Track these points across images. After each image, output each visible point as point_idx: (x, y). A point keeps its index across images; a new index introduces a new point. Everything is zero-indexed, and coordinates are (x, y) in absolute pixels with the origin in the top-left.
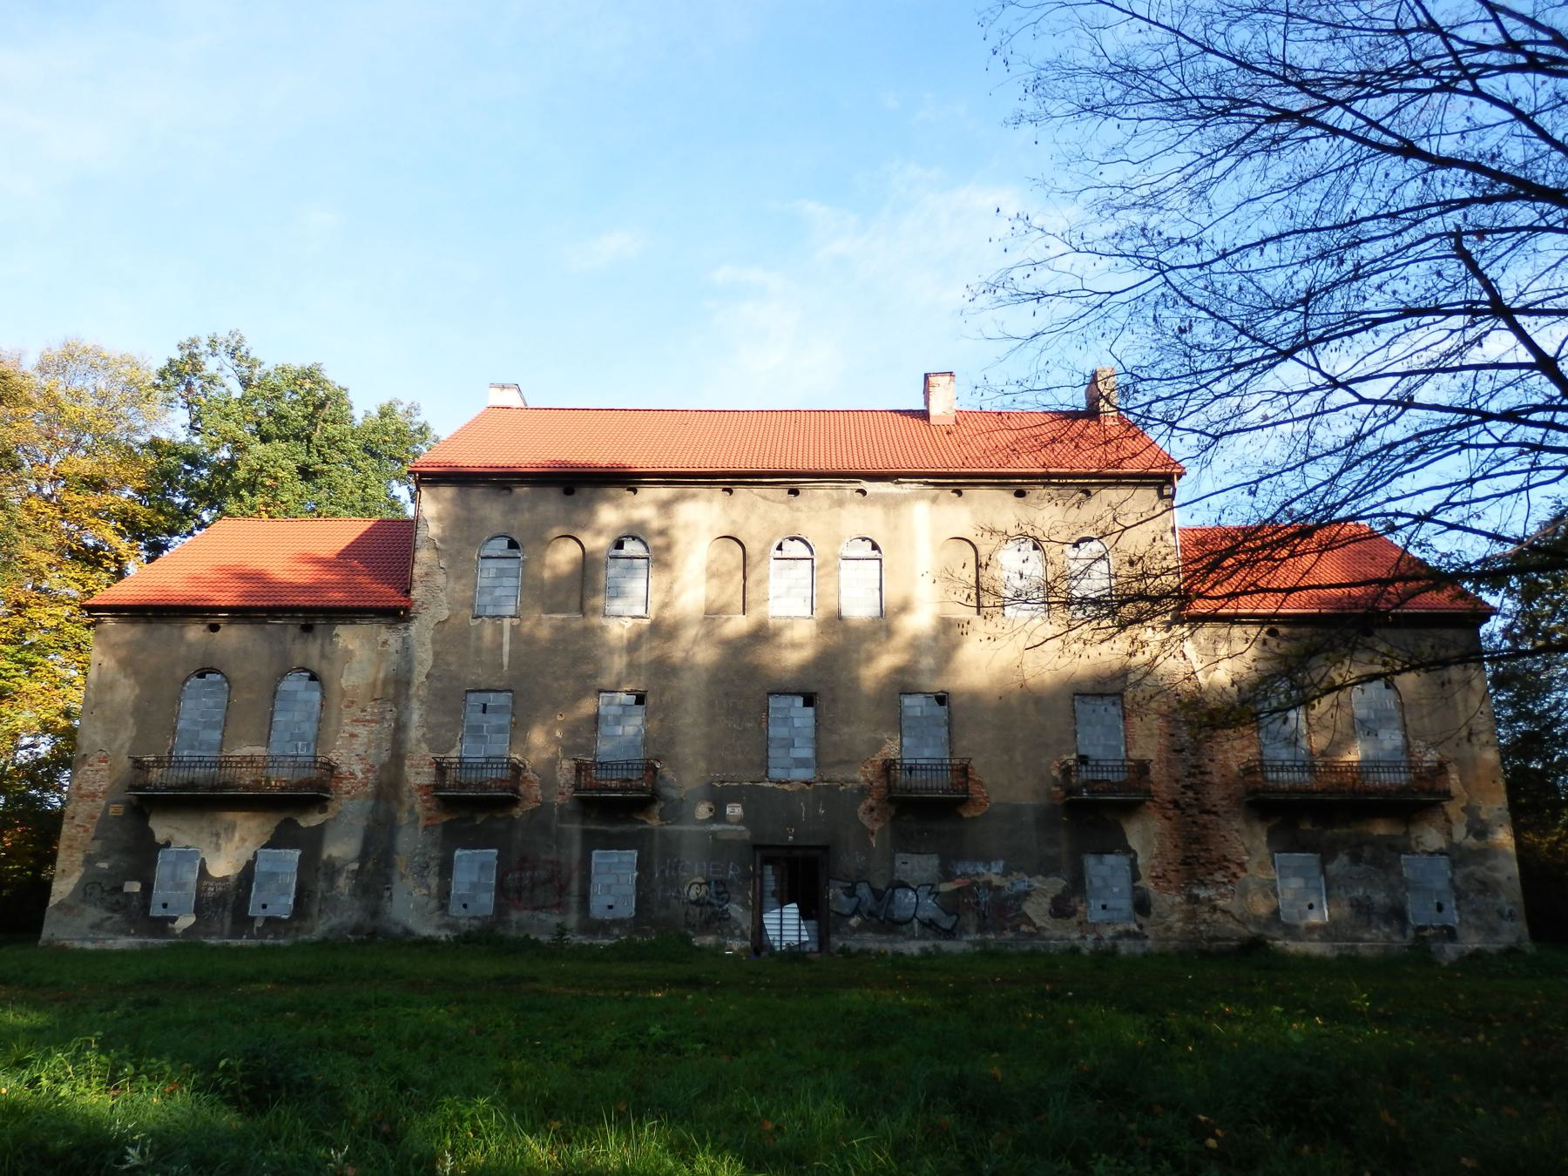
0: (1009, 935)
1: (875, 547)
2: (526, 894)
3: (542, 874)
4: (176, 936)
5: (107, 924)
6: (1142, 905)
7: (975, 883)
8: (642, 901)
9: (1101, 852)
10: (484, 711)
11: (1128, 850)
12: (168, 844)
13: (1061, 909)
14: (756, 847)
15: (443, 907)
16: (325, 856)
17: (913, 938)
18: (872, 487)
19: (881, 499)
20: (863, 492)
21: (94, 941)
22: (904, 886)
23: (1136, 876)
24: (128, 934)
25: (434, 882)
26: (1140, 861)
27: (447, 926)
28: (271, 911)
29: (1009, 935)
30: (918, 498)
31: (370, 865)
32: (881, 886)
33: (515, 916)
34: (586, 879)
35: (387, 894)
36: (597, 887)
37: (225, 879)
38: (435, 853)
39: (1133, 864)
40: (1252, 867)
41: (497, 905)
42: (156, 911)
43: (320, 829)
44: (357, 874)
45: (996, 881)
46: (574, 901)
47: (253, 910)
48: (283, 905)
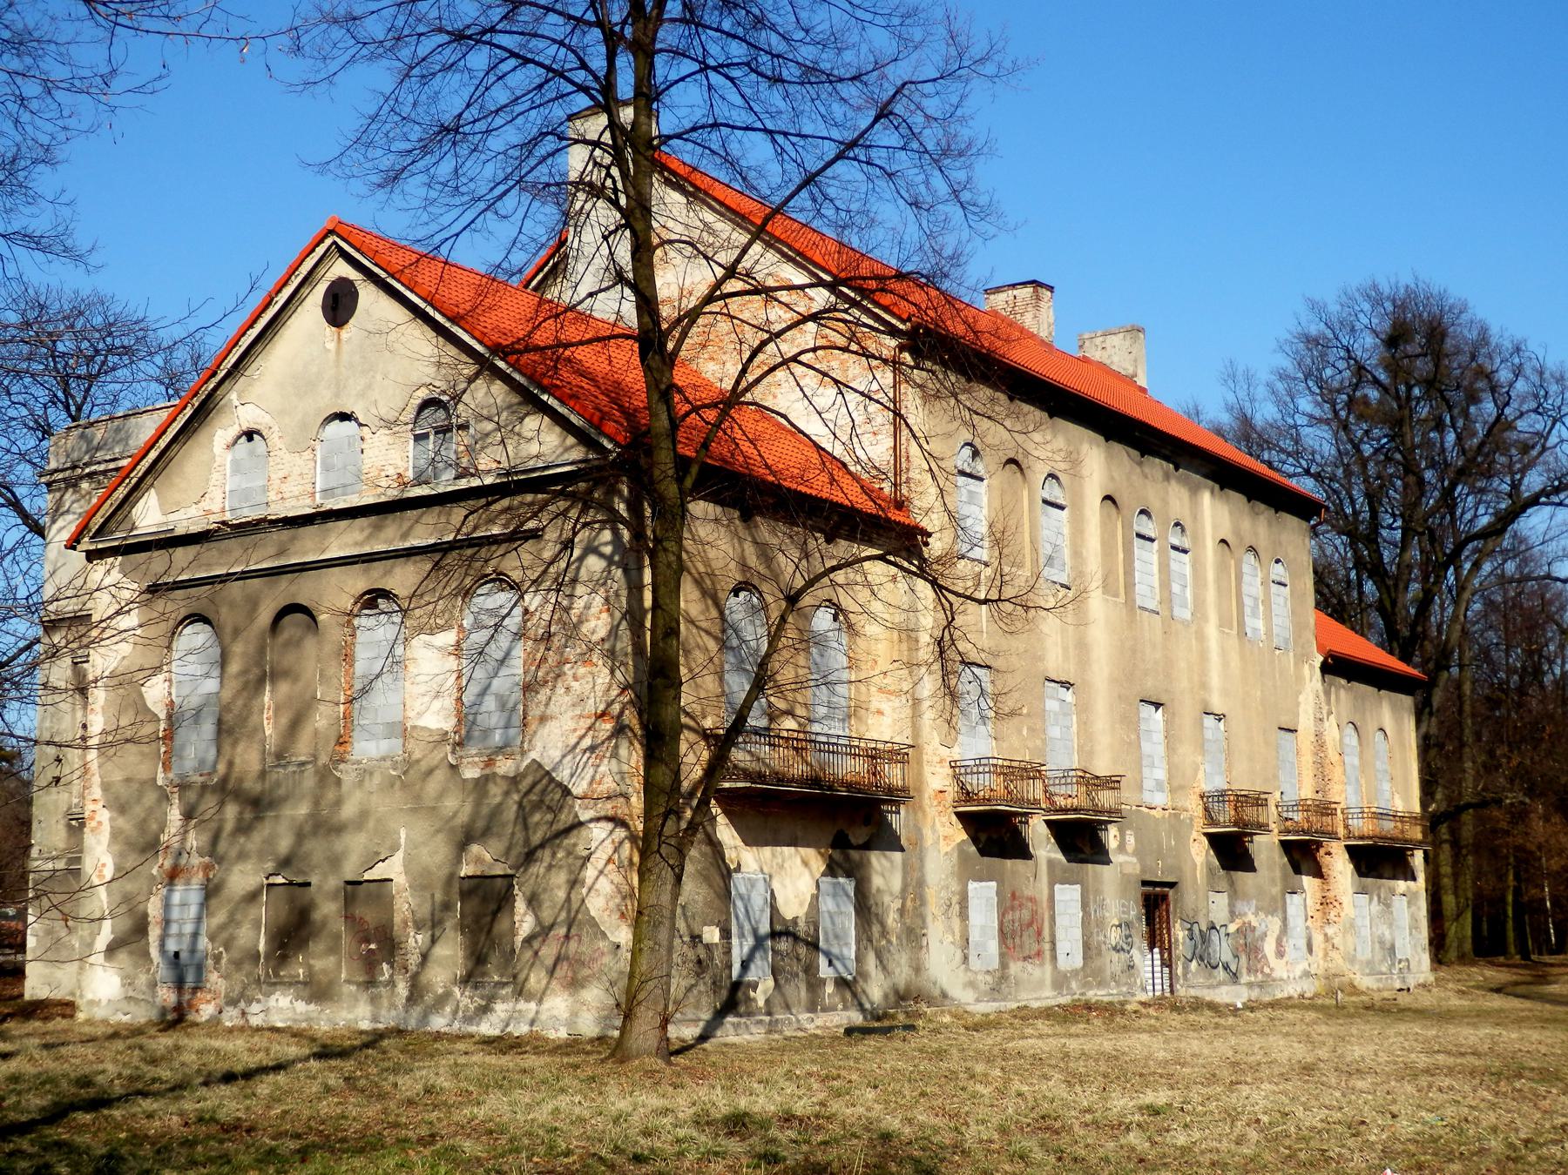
2: (1017, 940)
3: (1026, 914)
8: (1086, 946)
13: (1280, 954)
14: (1145, 883)
15: (966, 958)
33: (1015, 968)
36: (1060, 934)
38: (955, 887)
41: (1002, 955)
46: (1047, 946)
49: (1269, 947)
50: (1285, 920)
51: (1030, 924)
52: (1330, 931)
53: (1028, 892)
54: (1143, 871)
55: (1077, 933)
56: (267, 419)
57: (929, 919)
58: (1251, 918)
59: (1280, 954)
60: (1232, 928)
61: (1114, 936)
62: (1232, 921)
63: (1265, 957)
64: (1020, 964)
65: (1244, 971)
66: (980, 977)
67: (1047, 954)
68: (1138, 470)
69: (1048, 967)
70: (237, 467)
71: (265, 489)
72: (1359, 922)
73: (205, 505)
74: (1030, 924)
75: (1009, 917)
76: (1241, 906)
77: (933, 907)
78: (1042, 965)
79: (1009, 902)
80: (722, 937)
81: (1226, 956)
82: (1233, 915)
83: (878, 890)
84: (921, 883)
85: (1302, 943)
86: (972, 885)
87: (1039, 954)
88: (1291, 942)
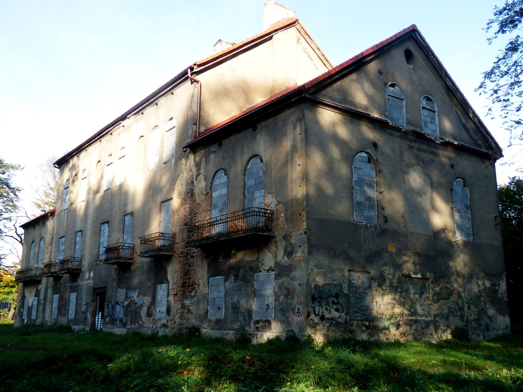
6: (168, 311)
7: (131, 301)
11: (168, 282)
13: (149, 314)
17: (117, 327)
29: (137, 325)
32: (113, 304)
39: (169, 286)
40: (201, 285)
46: (67, 312)
49: (143, 312)
50: (154, 298)
52: (187, 302)
53: (65, 297)
54: (94, 285)
55: (74, 308)
59: (149, 314)
60: (126, 303)
61: (83, 308)
62: (126, 300)
63: (140, 316)
65: (129, 323)
69: (66, 318)
79: (61, 299)
81: (121, 315)
82: (127, 298)
85: (164, 309)
87: (65, 314)
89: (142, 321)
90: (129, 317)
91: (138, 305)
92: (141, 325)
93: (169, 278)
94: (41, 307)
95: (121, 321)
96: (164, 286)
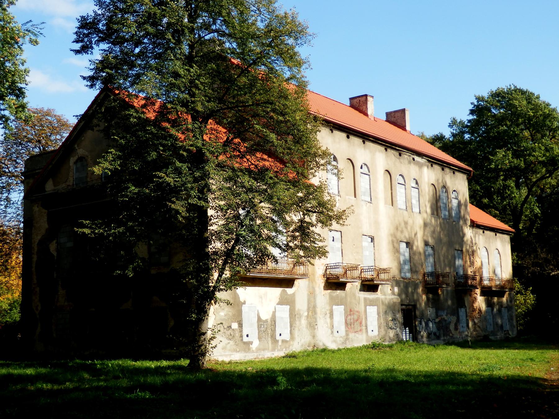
0: (448, 337)
1: (417, 183)
2: (352, 326)
3: (356, 317)
4: (253, 352)
5: (228, 346)
9: (461, 307)
10: (333, 241)
11: (466, 307)
12: (244, 303)
13: (456, 329)
16: (297, 309)
18: (417, 158)
19: (418, 164)
20: (414, 159)
21: (226, 356)
22: (429, 320)
23: (467, 317)
24: (237, 352)
25: (328, 320)
26: (467, 310)
27: (335, 341)
28: (283, 337)
29: (448, 337)
30: (425, 165)
31: (310, 313)
33: (351, 335)
34: (366, 318)
35: (316, 327)
36: (369, 323)
37: (266, 321)
38: (328, 308)
39: (466, 310)
41: (346, 331)
42: (245, 339)
43: (294, 294)
44: (308, 317)
45: (446, 318)
46: (364, 328)
47: (278, 337)
48: (286, 336)
49: (452, 327)
51: (357, 320)
53: (356, 309)
56: (87, 153)
57: (318, 319)
58: (445, 317)
59: (456, 329)
60: (437, 320)
62: (437, 318)
63: (450, 330)
64: (353, 334)
65: (442, 335)
66: (338, 339)
67: (364, 331)
68: (398, 160)
69: (364, 335)
70: (77, 169)
71: (87, 177)
72: (488, 317)
73: (68, 183)
74: (357, 320)
75: (349, 317)
76: (440, 313)
77: (319, 315)
78: (362, 334)
79: (349, 312)
80: (239, 326)
82: (437, 316)
83: (298, 310)
84: (315, 307)
86: (334, 307)
88: (461, 325)
89: (451, 333)
90: (442, 332)
91: (447, 322)
92: (452, 337)
93: (466, 305)
94: (304, 322)
95: (435, 334)
96: (463, 310)
